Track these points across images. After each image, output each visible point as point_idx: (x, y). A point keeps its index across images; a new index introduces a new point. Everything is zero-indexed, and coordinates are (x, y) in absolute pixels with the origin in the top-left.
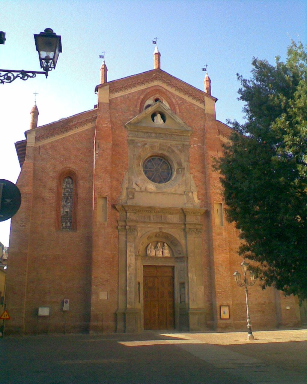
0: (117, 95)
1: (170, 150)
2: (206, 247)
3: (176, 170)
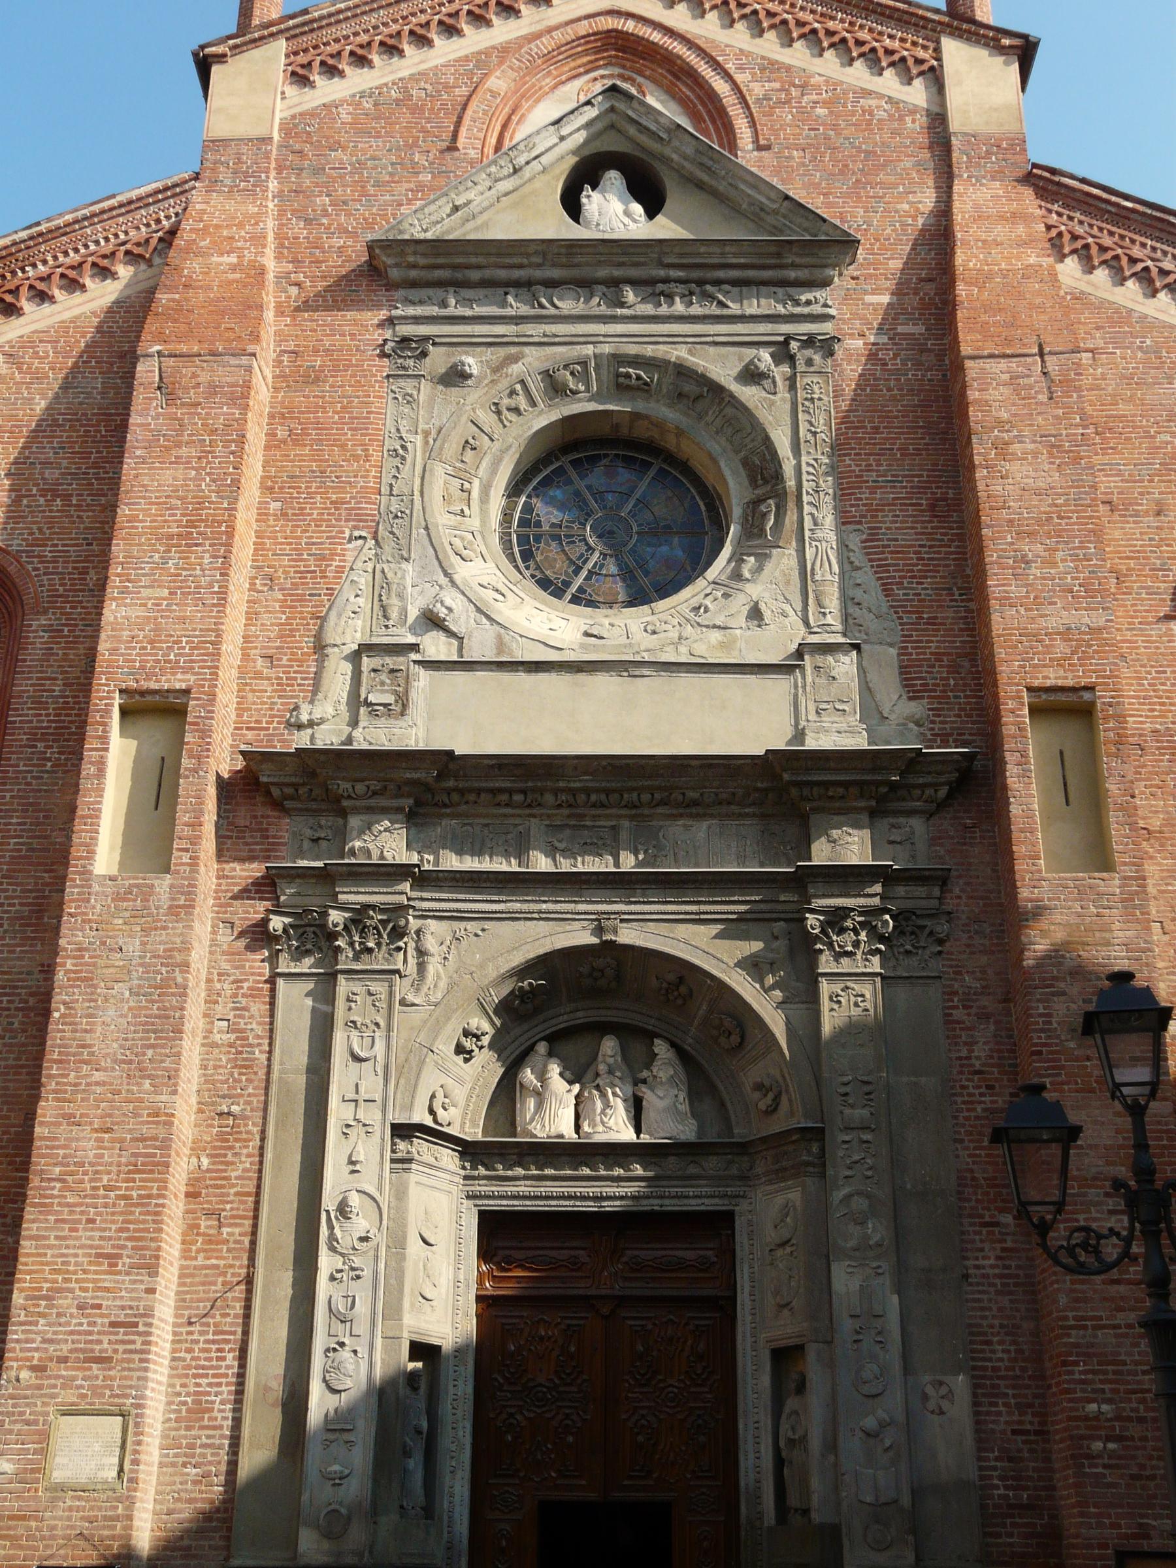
0: (326, 90)
1: (689, 388)
2: (981, 1051)
3: (737, 512)
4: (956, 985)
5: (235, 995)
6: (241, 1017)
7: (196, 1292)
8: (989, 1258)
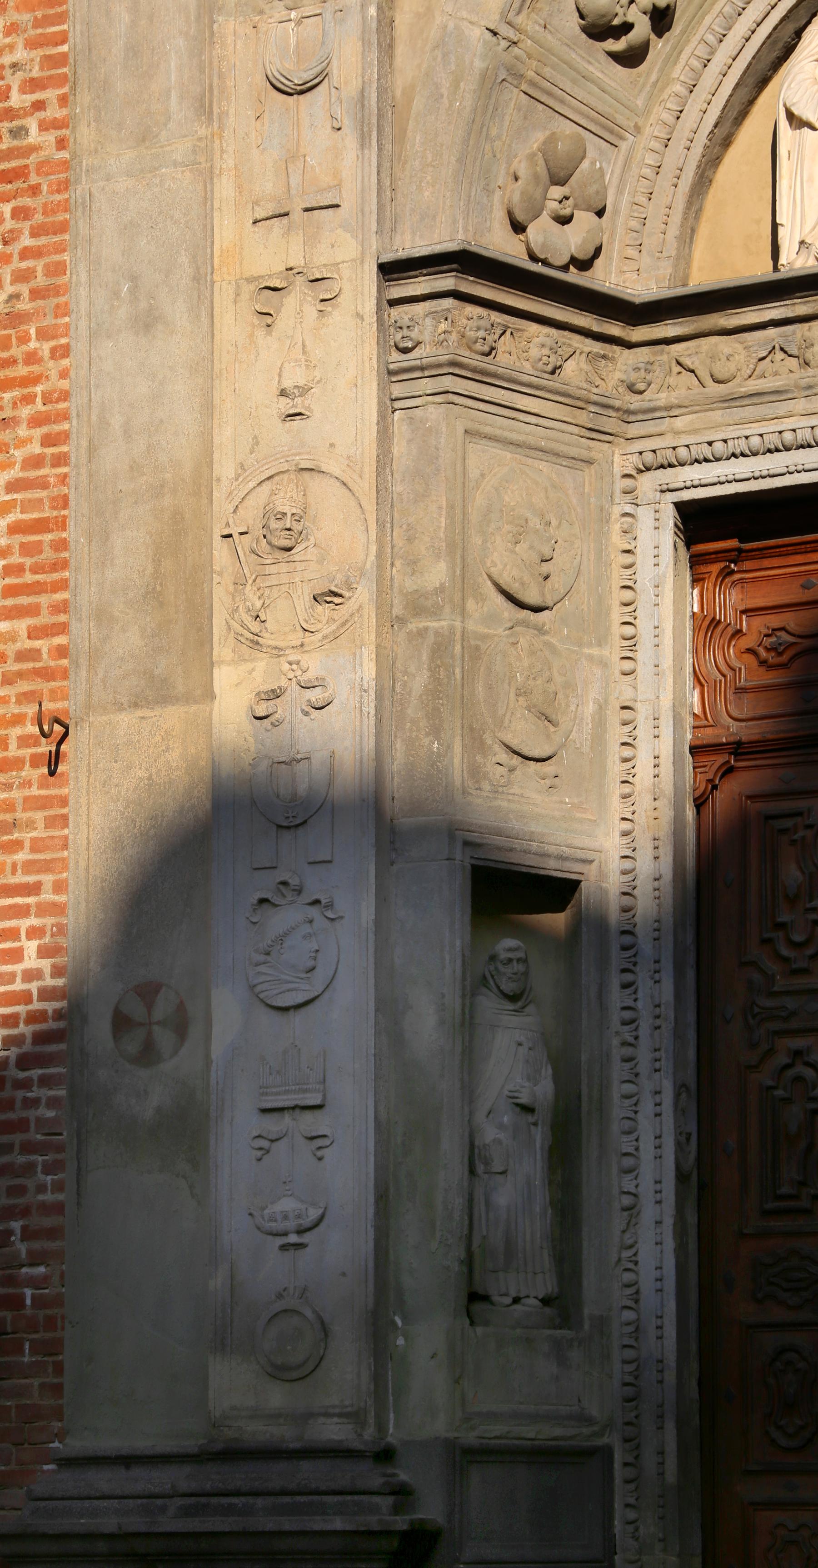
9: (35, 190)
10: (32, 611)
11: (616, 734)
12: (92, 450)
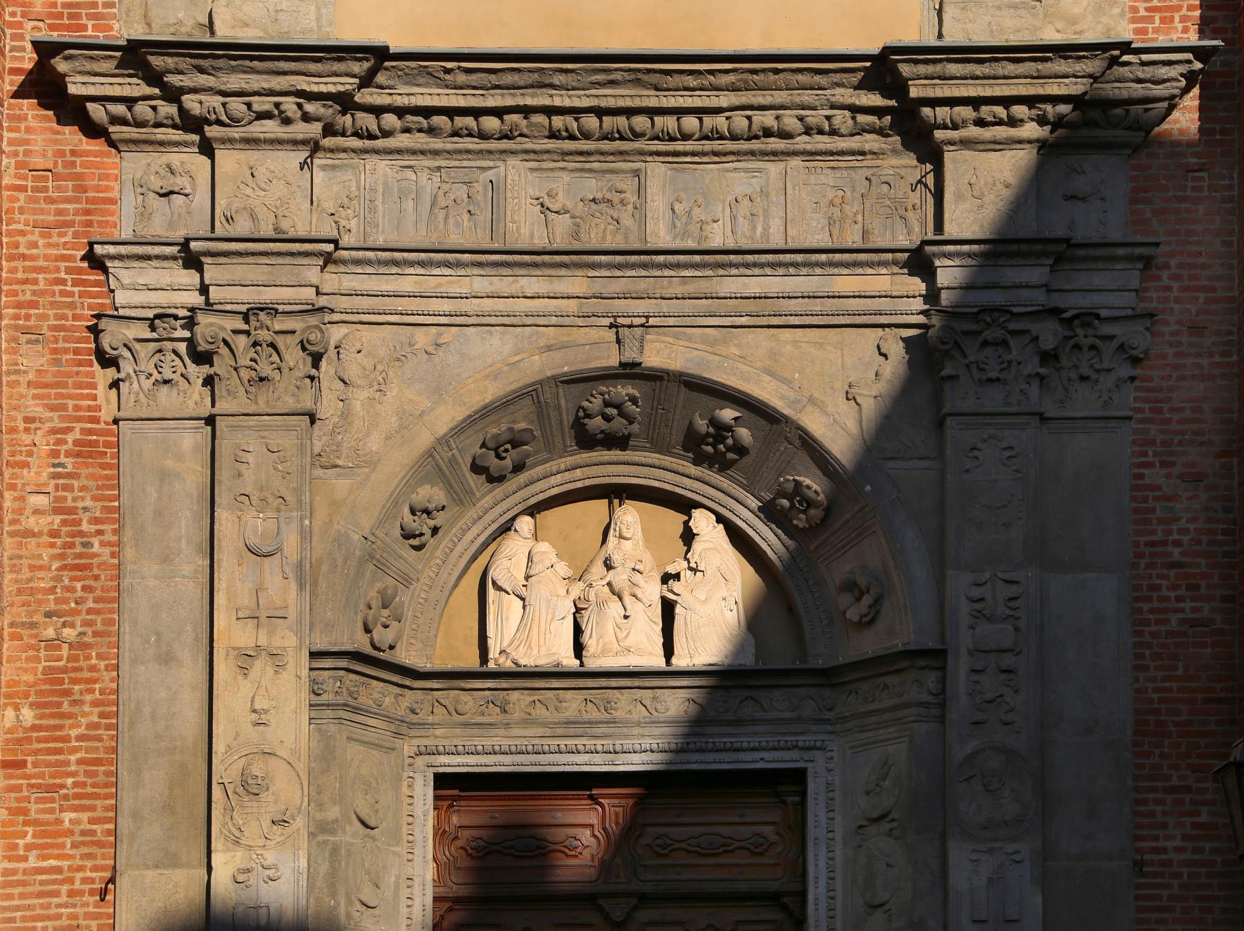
4: (1153, 429)
5: (55, 454)
6: (67, 488)
7: (29, 907)
8: (1174, 838)
9: (97, 578)
10: (92, 808)
11: (404, 892)
12: (132, 724)
